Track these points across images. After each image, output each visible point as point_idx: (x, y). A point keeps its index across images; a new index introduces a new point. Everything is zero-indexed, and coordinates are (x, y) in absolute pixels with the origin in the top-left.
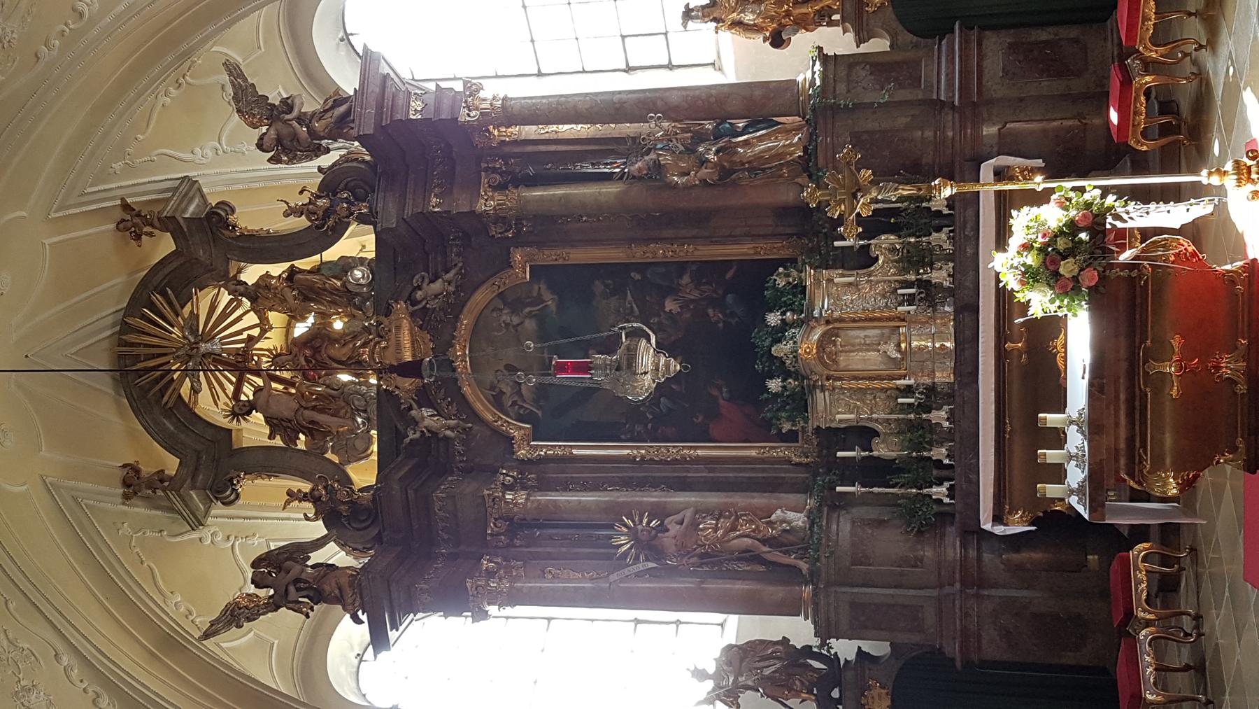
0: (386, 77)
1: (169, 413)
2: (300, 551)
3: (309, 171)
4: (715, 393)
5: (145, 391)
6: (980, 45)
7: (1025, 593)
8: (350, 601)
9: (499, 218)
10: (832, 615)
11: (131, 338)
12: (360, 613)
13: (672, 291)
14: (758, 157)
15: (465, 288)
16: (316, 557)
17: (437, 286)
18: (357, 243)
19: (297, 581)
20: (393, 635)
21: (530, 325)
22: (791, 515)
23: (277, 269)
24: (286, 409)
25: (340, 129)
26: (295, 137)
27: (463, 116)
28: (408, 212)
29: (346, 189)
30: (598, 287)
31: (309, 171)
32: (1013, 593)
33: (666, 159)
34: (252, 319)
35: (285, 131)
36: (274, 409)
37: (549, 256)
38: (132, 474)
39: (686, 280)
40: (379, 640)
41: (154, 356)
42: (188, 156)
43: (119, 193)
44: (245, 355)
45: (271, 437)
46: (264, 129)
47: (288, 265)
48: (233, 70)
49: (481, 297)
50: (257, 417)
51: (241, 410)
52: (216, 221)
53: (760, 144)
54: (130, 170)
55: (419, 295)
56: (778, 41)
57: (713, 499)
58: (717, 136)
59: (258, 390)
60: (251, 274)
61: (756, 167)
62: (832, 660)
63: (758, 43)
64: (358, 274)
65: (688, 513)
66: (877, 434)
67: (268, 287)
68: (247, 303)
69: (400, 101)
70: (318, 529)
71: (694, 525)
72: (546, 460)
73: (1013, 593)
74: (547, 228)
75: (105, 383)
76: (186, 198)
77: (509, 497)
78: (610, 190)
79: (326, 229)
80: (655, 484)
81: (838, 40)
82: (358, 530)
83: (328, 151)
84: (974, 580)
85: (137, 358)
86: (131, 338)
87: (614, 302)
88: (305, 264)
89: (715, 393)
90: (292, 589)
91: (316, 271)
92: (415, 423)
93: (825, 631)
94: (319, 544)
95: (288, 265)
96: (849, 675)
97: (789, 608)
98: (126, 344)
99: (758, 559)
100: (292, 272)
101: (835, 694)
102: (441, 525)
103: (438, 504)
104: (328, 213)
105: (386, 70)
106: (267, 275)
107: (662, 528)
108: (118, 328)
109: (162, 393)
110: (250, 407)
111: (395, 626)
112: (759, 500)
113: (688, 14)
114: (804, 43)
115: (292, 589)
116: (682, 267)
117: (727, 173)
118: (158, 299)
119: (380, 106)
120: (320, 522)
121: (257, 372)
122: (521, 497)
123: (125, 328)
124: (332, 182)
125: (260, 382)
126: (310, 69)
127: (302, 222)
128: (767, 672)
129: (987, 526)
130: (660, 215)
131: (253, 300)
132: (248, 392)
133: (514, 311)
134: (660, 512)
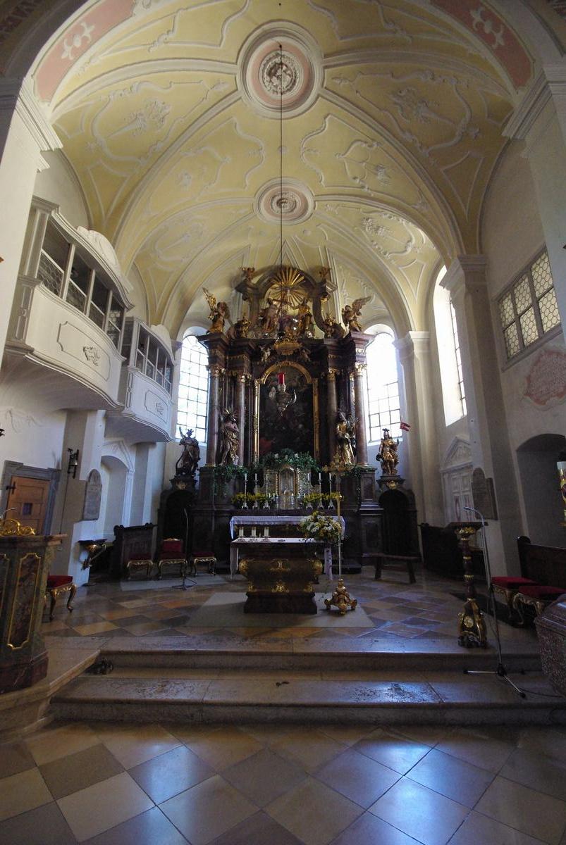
0: (367, 341)
1: (269, 281)
2: (227, 316)
3: (340, 320)
4: (274, 439)
5: (276, 274)
6: (376, 516)
7: (213, 529)
9: (327, 374)
11: (291, 270)
13: (305, 426)
14: (345, 451)
15: (306, 365)
16: (226, 321)
17: (307, 356)
18: (319, 334)
19: (219, 315)
20: (203, 342)
21: (295, 384)
22: (237, 461)
23: (311, 311)
24: (271, 313)
25: (352, 328)
26: (350, 316)
27: (357, 365)
28: (328, 347)
29: (335, 331)
30: (306, 404)
31: (340, 320)
32: (213, 526)
33: (345, 424)
34: (296, 304)
35: (352, 313)
36: (271, 310)
37: (315, 390)
39: (308, 430)
40: (200, 338)
41: (286, 277)
42: (344, 287)
43: (333, 268)
44: (286, 302)
45: (263, 310)
46: (351, 306)
47: (312, 314)
48: (369, 299)
49: (303, 370)
50: (268, 306)
51: (270, 302)
52: (325, 294)
53: (349, 452)
54: (340, 271)
55: (304, 351)
56: (378, 457)
57: (242, 438)
58: (352, 439)
59: (276, 306)
60: (310, 304)
61: (343, 450)
63: (378, 452)
64: (310, 334)
65: (238, 430)
66: (261, 486)
67: (306, 308)
68: (301, 303)
69: (361, 346)
70: (235, 322)
71: (234, 431)
72: (254, 388)
73: (213, 526)
74: (324, 390)
75: (278, 263)
76: (331, 287)
77: (243, 377)
78: (335, 407)
79: (323, 325)
80: (247, 421)
81: (378, 474)
83: (346, 326)
84: (218, 514)
85: (285, 273)
86: (291, 270)
87: (301, 409)
88: (313, 319)
89: (274, 439)
91: (311, 323)
92: (266, 349)
93: (201, 470)
95: (312, 314)
96: (189, 478)
97: (209, 460)
98: (289, 269)
99: (223, 452)
100: (311, 316)
101: (184, 473)
103: (241, 356)
104: (328, 325)
105: (370, 342)
106: (309, 309)
107: (233, 422)
108: (293, 266)
109: (275, 279)
110: (270, 303)
111: (205, 343)
112: (242, 452)
113: (386, 430)
114: (377, 465)
116: (312, 429)
117: (342, 441)
118: (303, 278)
119: (359, 339)
121: (281, 305)
122: (243, 381)
123: (294, 269)
124: (337, 326)
125: (278, 306)
126: (371, 322)
127: (324, 318)
129: (233, 519)
130: (328, 422)
131: (302, 305)
132: (275, 303)
133: (299, 379)
134: (238, 422)
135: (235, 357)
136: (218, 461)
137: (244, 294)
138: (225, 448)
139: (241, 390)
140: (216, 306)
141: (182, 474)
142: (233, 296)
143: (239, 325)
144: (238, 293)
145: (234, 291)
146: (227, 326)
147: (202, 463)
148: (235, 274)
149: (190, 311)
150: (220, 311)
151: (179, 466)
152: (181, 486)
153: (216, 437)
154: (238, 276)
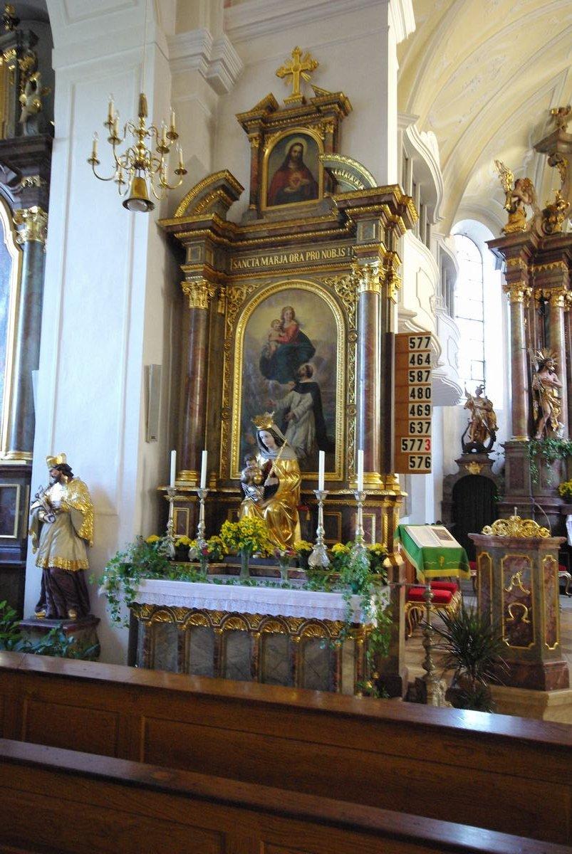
2: (532, 200)
8: (511, 227)
10: (516, 450)
12: (504, 232)
20: (495, 249)
38: (565, 110)
62: (489, 449)
70: (542, 207)
82: (542, 226)
90: (516, 199)
94: (535, 208)
96: (484, 457)
97: (516, 429)
102: (546, 267)
103: (557, 264)
115: (516, 199)
120: (545, 208)
122: (561, 304)
128: (483, 421)
134: (557, 371)
135: (546, 267)
136: (532, 432)
137: (551, 156)
138: (541, 412)
139: (558, 321)
140: (511, 187)
141: (471, 452)
142: (528, 160)
143: (549, 213)
144: (539, 154)
145: (531, 153)
146: (530, 213)
147: (503, 435)
148: (536, 123)
149: (465, 194)
150: (520, 193)
151: (467, 440)
152: (473, 469)
153: (525, 397)
154: (539, 127)
